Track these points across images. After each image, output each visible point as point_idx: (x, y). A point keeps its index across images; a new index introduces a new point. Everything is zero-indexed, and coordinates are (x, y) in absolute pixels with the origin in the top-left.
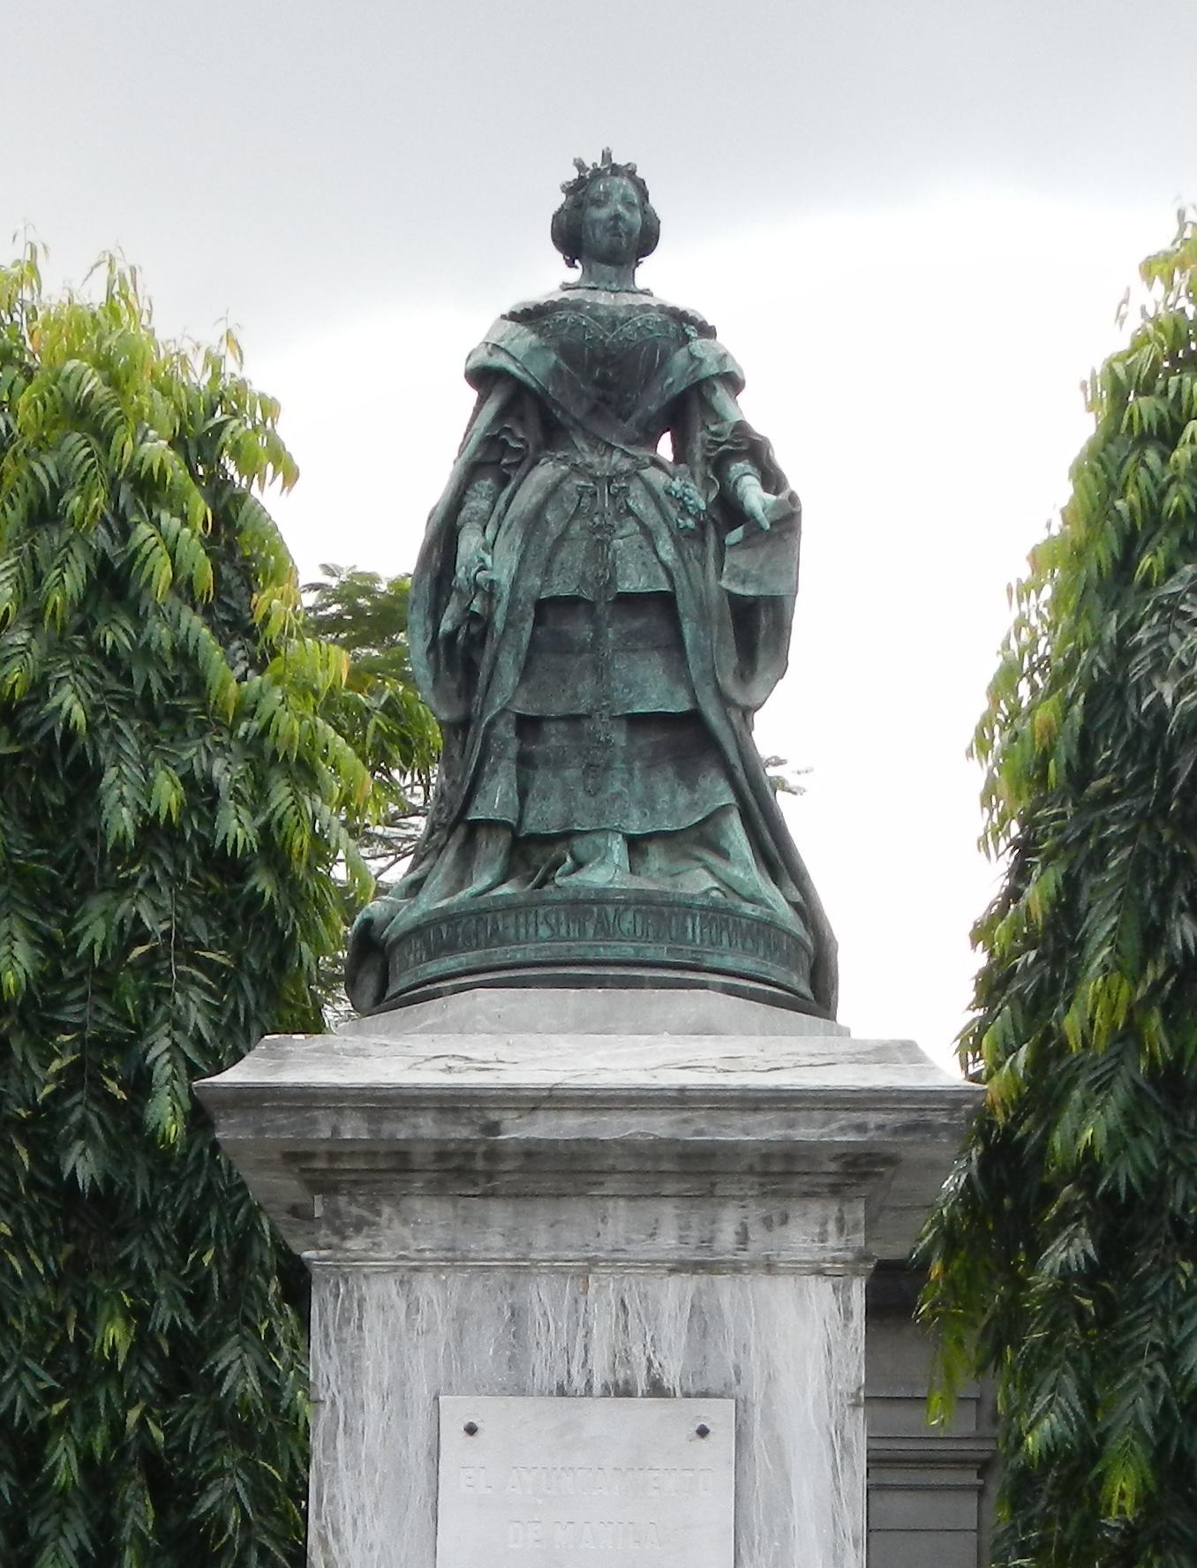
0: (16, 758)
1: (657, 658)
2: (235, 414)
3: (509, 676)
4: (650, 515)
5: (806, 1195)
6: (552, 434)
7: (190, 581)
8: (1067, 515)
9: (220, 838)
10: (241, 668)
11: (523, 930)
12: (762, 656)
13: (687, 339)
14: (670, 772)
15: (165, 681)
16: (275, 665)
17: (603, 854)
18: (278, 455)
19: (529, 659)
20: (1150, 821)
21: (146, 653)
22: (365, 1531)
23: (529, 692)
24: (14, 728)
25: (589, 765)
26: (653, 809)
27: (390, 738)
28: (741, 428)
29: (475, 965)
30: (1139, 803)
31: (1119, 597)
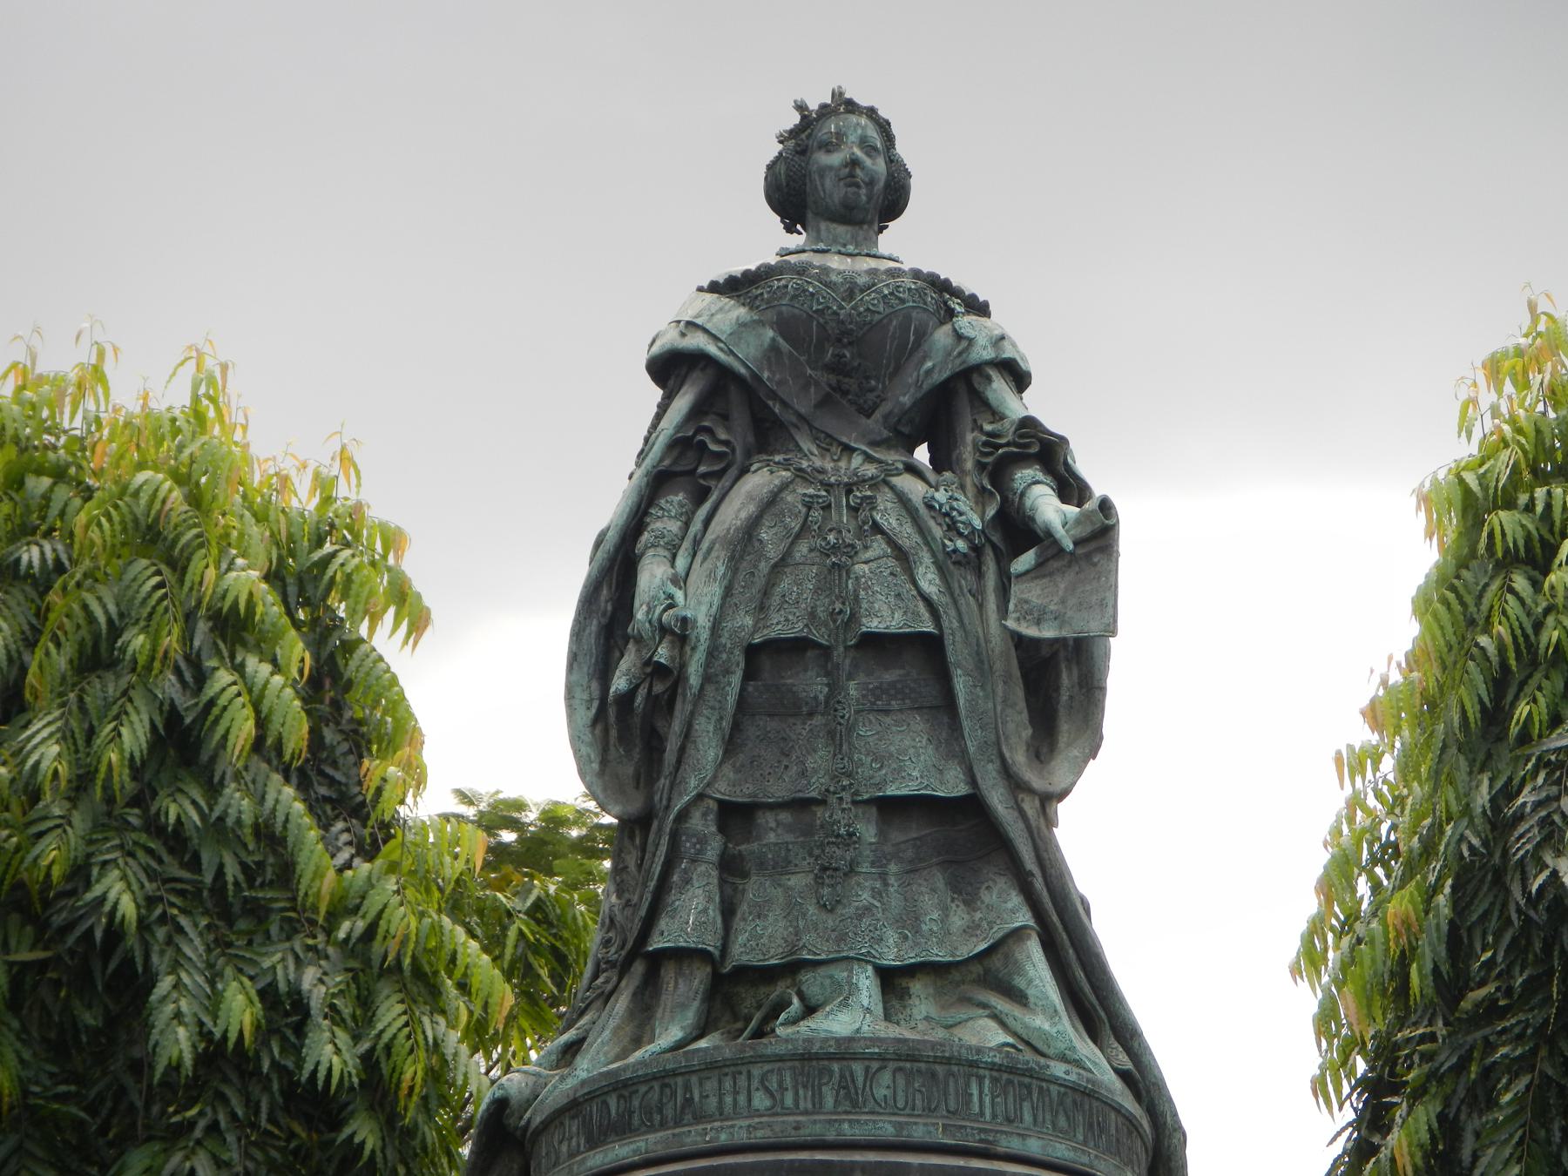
0: (42, 966)
1: (918, 723)
2: (347, 545)
3: (708, 749)
4: (906, 534)
6: (768, 434)
7: (279, 746)
8: (1414, 660)
9: (309, 1067)
10: (344, 856)
11: (728, 1100)
12: (1065, 728)
13: (951, 314)
14: (939, 880)
15: (244, 867)
16: (389, 851)
17: (844, 994)
18: (402, 595)
19: (736, 727)
20: (1551, 1042)
21: (219, 829)
23: (738, 771)
24: (41, 925)
25: (824, 869)
26: (917, 931)
27: (536, 949)
28: (1029, 425)
29: (661, 1151)
30: (1535, 1017)
31: (1489, 756)
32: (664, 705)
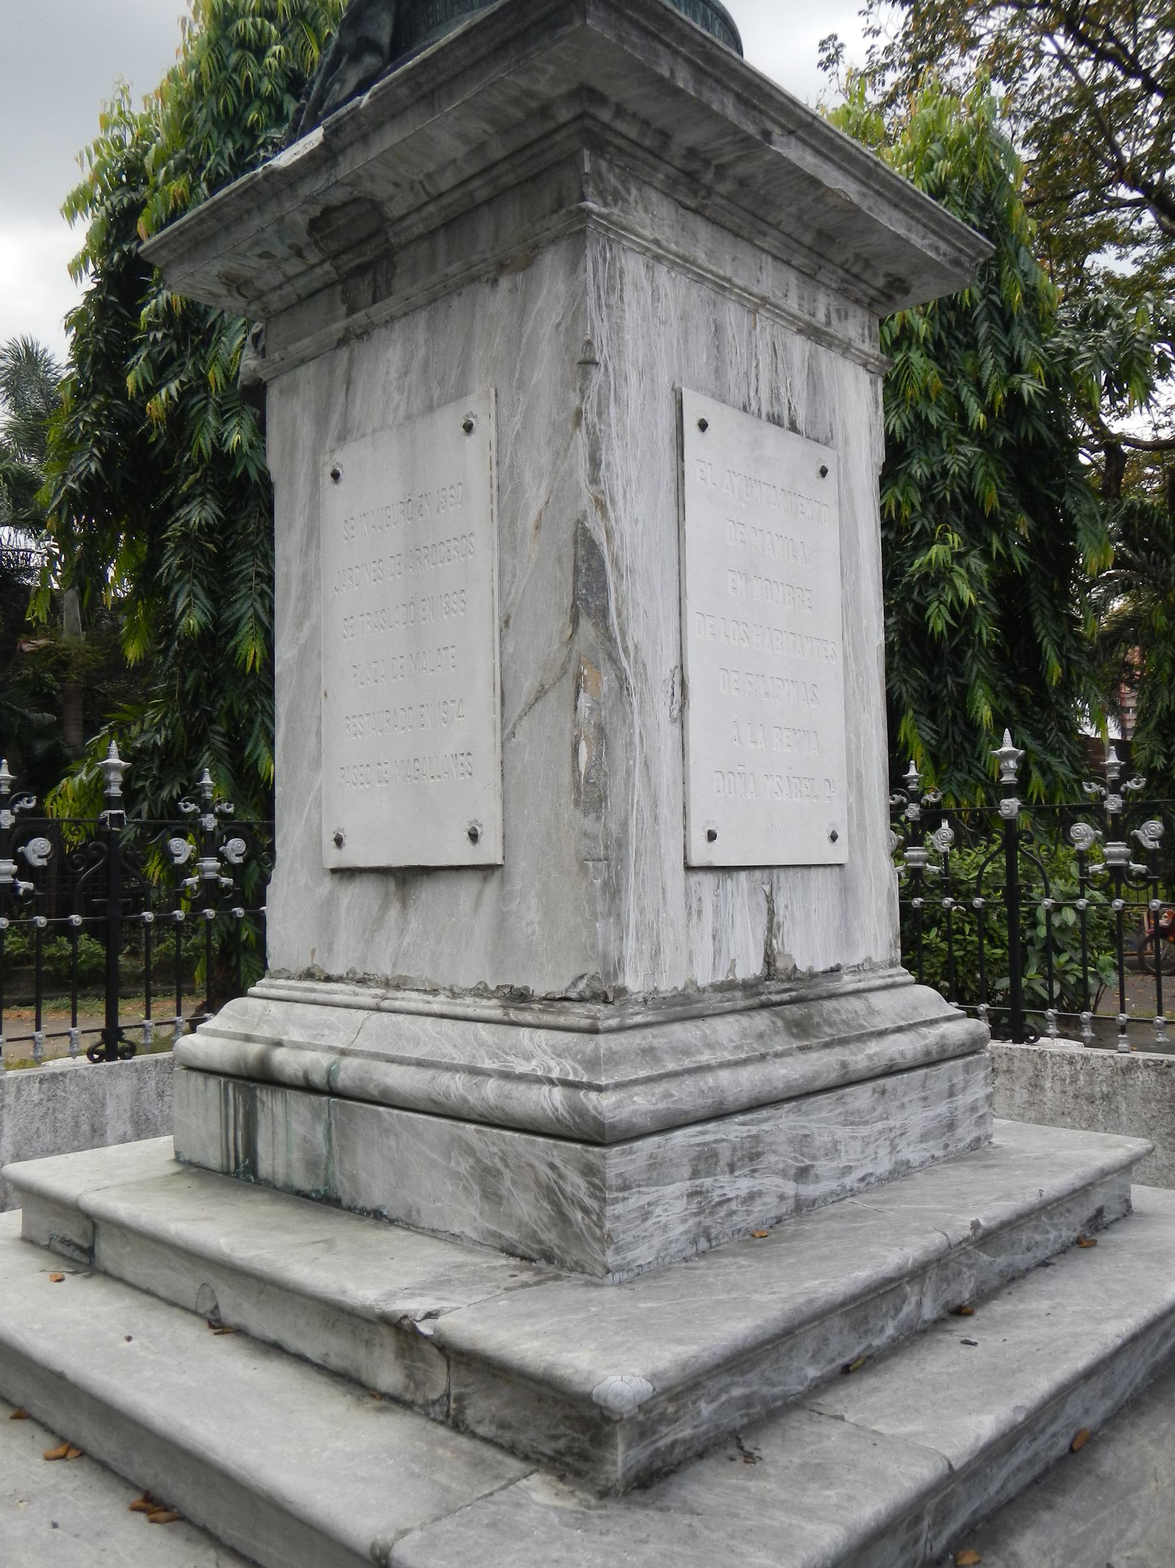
5: (857, 301)
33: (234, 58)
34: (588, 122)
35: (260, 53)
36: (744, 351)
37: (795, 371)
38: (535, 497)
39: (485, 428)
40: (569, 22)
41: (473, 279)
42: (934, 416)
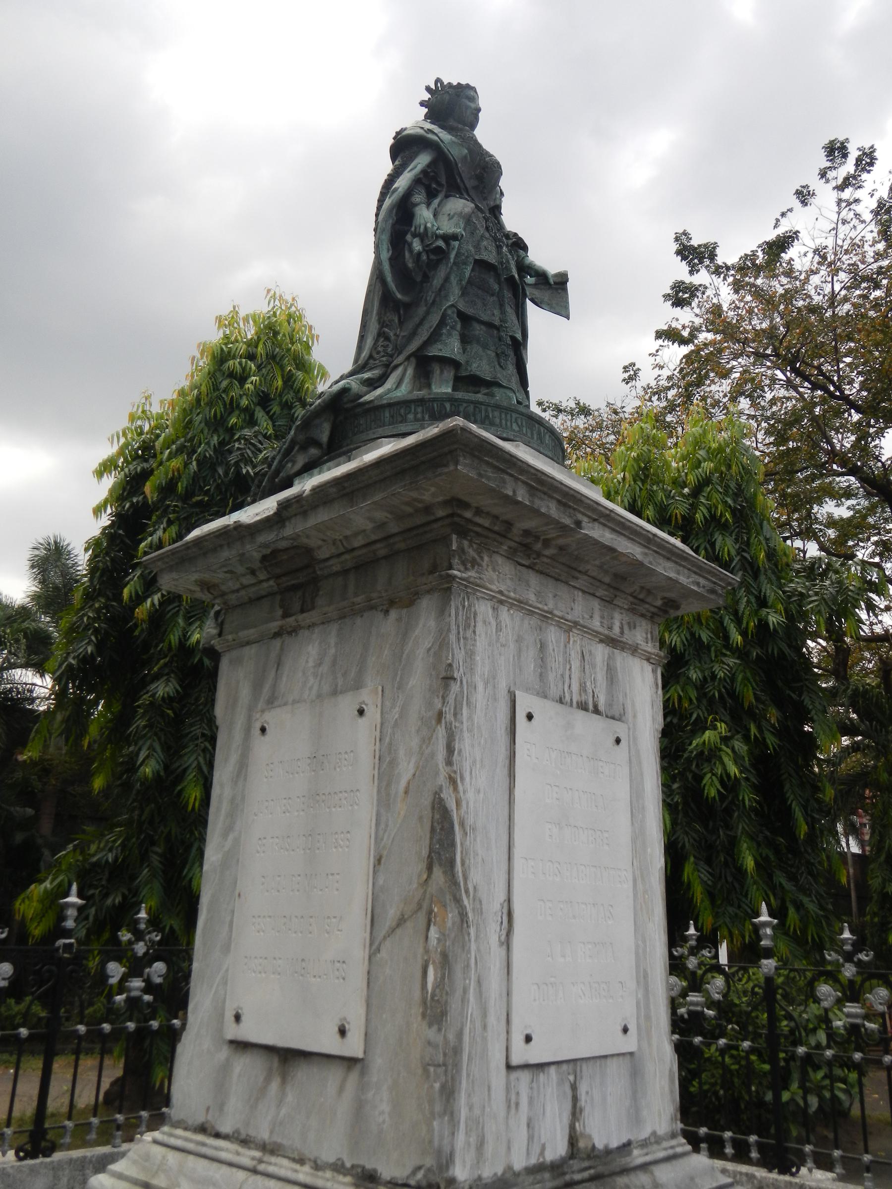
5: (643, 616)
11: (504, 422)
22: (476, 778)
32: (433, 265)
33: (225, 384)
34: (456, 519)
35: (242, 379)
36: (561, 659)
37: (598, 669)
38: (406, 770)
39: (373, 713)
40: (446, 466)
41: (372, 608)
42: (705, 636)
